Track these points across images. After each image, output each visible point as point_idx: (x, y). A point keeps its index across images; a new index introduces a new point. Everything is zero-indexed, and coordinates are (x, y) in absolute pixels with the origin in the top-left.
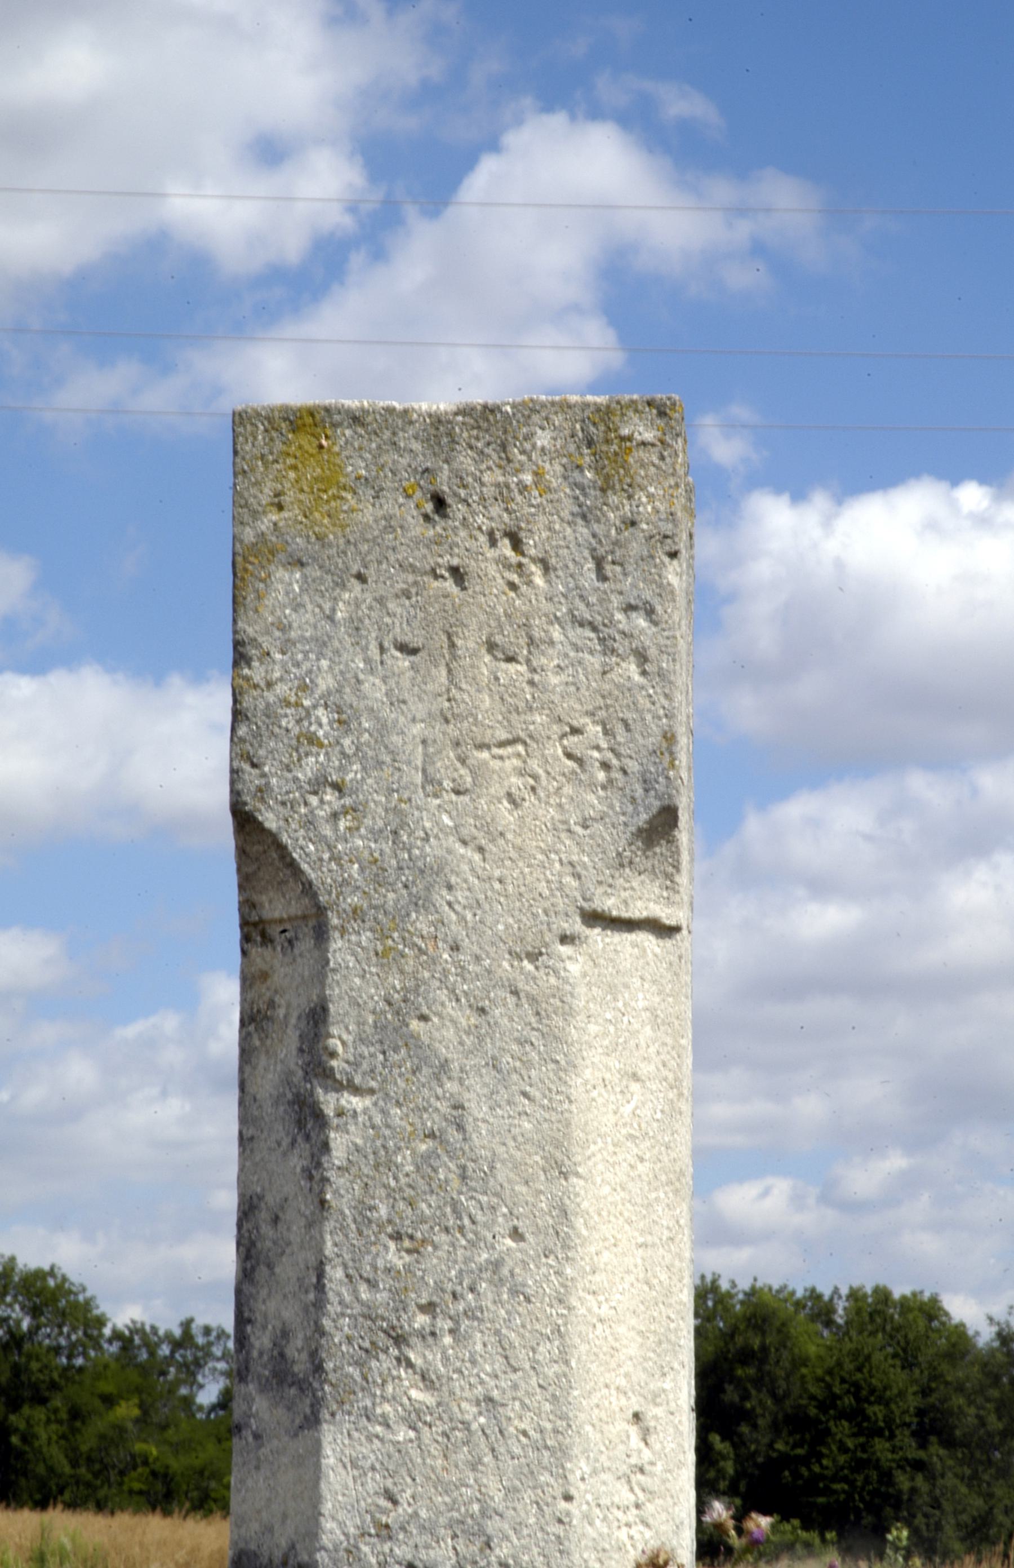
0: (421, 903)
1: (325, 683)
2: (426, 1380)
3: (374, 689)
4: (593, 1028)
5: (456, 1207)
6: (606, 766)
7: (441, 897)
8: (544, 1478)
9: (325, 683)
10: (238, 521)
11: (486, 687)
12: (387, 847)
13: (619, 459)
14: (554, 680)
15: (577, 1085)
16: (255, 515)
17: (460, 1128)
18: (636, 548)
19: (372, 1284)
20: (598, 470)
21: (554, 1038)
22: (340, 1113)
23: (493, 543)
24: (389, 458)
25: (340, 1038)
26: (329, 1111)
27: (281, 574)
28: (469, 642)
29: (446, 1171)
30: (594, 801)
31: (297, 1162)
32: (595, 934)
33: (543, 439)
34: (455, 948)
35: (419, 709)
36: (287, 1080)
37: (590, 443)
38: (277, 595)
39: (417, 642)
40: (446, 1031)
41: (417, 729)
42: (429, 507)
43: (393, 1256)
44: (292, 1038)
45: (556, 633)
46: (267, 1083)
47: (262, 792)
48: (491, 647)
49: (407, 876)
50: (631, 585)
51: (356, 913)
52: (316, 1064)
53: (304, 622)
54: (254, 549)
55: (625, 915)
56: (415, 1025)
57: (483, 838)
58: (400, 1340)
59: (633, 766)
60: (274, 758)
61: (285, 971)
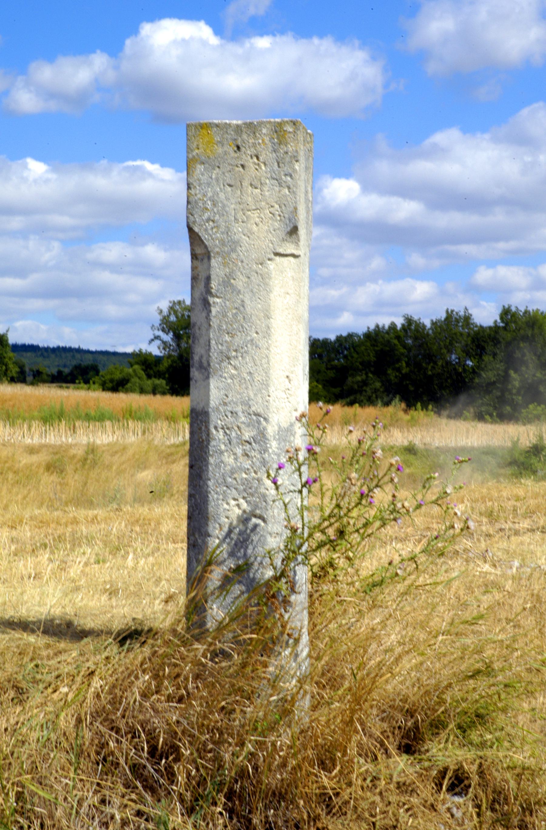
0: (234, 250)
1: (210, 194)
2: (235, 368)
3: (222, 196)
4: (276, 282)
5: (242, 327)
6: (280, 216)
7: (239, 249)
8: (263, 391)
9: (210, 194)
10: (188, 152)
11: (250, 195)
12: (225, 236)
13: (283, 136)
14: (267, 193)
15: (272, 296)
16: (192, 151)
17: (243, 306)
18: (288, 159)
19: (222, 345)
20: (278, 139)
21: (266, 284)
22: (214, 303)
23: (252, 157)
24: (226, 136)
25: (214, 284)
26: (211, 302)
27: (198, 166)
28: (246, 183)
29: (240, 317)
30: (277, 225)
31: (204, 314)
32: (277, 258)
33: (264, 131)
34: (242, 262)
35: (233, 201)
36: (202, 294)
37: (276, 132)
38: (198, 171)
39: (232, 183)
40: (240, 282)
41: (233, 206)
42: (236, 149)
43: (227, 338)
44: (203, 284)
45: (267, 181)
46: (197, 295)
47: (194, 222)
48: (251, 185)
49: (230, 243)
50: (287, 169)
51: (218, 253)
52: (208, 290)
53: (204, 179)
54: (192, 160)
55: (285, 253)
56: (232, 281)
57: (249, 234)
58: (229, 358)
59: (286, 216)
60: (197, 213)
61: (201, 267)
